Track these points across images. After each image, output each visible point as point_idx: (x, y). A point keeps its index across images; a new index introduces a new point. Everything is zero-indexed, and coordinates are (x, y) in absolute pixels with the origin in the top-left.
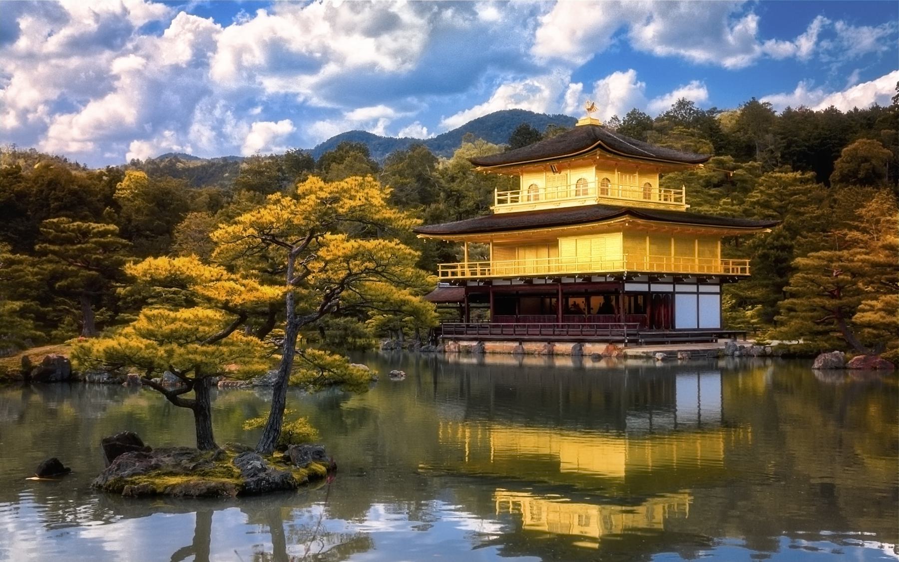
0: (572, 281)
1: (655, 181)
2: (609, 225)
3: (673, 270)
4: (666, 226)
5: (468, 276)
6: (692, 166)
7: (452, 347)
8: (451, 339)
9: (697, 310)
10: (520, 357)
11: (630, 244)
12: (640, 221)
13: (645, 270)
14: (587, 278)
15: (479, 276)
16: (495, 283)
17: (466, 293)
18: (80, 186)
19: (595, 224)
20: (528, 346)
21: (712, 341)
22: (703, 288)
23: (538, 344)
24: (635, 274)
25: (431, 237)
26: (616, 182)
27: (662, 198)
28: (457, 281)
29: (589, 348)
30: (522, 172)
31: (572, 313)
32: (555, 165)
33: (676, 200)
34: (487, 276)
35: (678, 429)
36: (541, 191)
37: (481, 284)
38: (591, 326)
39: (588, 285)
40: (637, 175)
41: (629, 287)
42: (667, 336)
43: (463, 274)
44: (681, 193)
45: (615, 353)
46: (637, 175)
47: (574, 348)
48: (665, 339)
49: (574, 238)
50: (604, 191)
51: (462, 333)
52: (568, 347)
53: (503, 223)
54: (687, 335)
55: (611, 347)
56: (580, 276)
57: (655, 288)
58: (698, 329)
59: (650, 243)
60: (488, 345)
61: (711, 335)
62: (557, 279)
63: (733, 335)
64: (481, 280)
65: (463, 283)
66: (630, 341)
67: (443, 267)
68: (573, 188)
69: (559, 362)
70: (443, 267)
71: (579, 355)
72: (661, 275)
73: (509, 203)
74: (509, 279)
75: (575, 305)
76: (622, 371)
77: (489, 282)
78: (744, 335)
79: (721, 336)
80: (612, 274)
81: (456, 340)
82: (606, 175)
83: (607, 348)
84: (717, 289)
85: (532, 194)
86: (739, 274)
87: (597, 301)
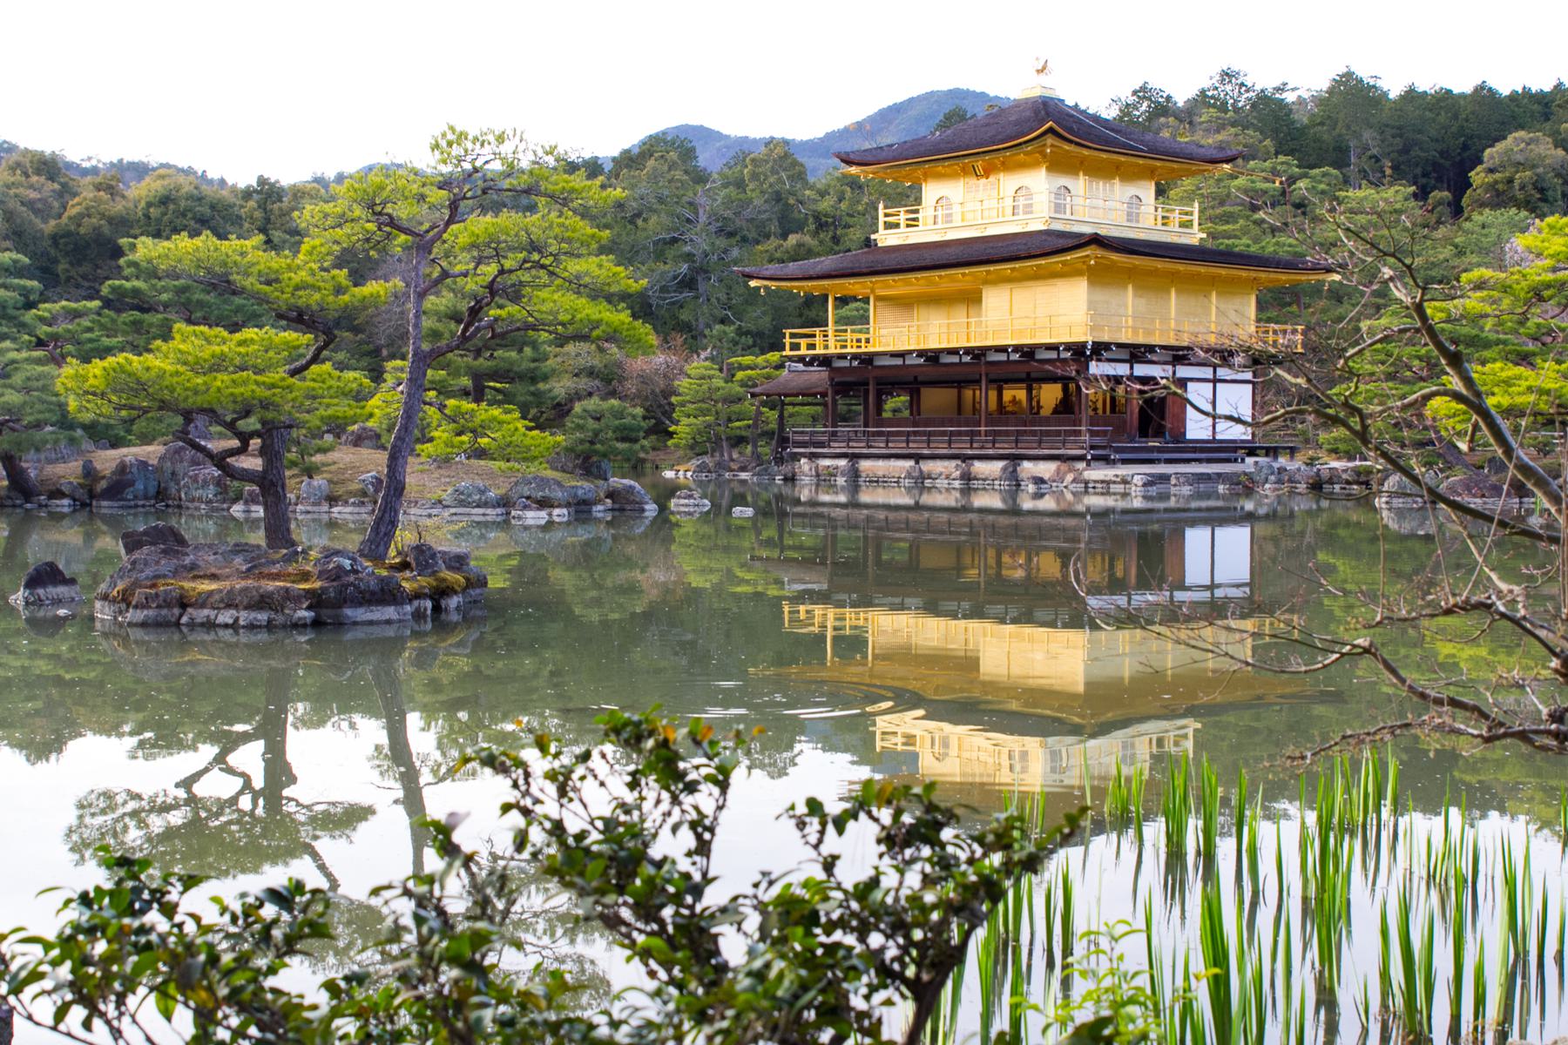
0: (1002, 357)
1: (1147, 191)
2: (1064, 263)
3: (1173, 342)
4: (1159, 264)
5: (832, 351)
6: (1210, 167)
7: (806, 468)
8: (803, 455)
11: (1102, 295)
12: (1115, 257)
13: (1124, 340)
14: (1028, 352)
16: (879, 362)
17: (832, 379)
18: (213, 207)
19: (1042, 262)
20: (927, 466)
21: (1236, 460)
22: (1222, 372)
23: (946, 463)
24: (1106, 346)
25: (773, 285)
26: (1081, 192)
27: (1160, 221)
28: (814, 358)
30: (926, 176)
32: (979, 165)
33: (1182, 225)
34: (863, 350)
36: (956, 210)
37: (855, 363)
38: (1034, 433)
39: (1027, 364)
40: (1117, 181)
42: (1159, 450)
43: (826, 347)
44: (1191, 214)
45: (1070, 477)
46: (1117, 181)
47: (1004, 469)
48: (1155, 455)
49: (1009, 286)
50: (1059, 208)
51: (821, 445)
53: (891, 261)
54: (1195, 450)
55: (1064, 467)
56: (1017, 348)
57: (1141, 370)
58: (1214, 440)
59: (1135, 295)
60: (865, 464)
61: (1235, 450)
62: (978, 353)
63: (1272, 452)
64: (855, 356)
65: (825, 361)
66: (1096, 458)
67: (793, 336)
68: (1009, 202)
70: (793, 336)
72: (1151, 348)
73: (903, 228)
74: (901, 355)
75: (1014, 401)
77: (867, 359)
78: (1292, 451)
79: (1252, 452)
80: (1069, 347)
81: (813, 457)
82: (1064, 181)
83: (1058, 470)
85: (939, 213)
87: (1050, 395)
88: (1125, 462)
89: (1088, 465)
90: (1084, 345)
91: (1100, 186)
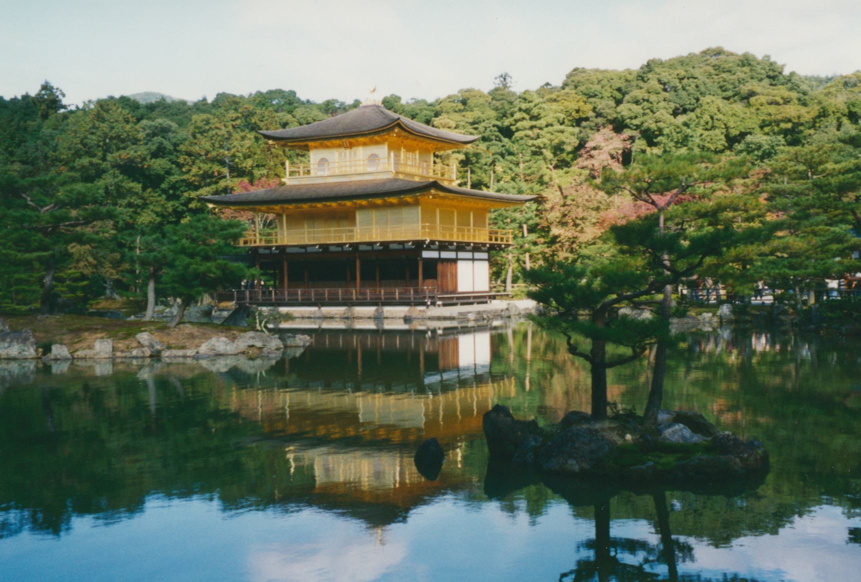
9: (472, 275)
10: (318, 321)
12: (441, 194)
15: (274, 244)
16: (288, 250)
20: (326, 310)
21: (486, 302)
22: (478, 255)
29: (388, 310)
31: (368, 278)
32: (346, 141)
35: (463, 383)
40: (417, 152)
41: (426, 254)
42: (458, 298)
43: (255, 242)
46: (417, 152)
47: (377, 310)
48: (455, 301)
52: (370, 310)
54: (469, 298)
55: (413, 308)
56: (382, 243)
57: (445, 255)
69: (359, 325)
71: (378, 318)
72: (451, 243)
76: (424, 332)
77: (282, 249)
84: (485, 255)
86: (505, 242)
88: (444, 305)
89: (428, 306)
90: (423, 242)
91: (410, 155)
